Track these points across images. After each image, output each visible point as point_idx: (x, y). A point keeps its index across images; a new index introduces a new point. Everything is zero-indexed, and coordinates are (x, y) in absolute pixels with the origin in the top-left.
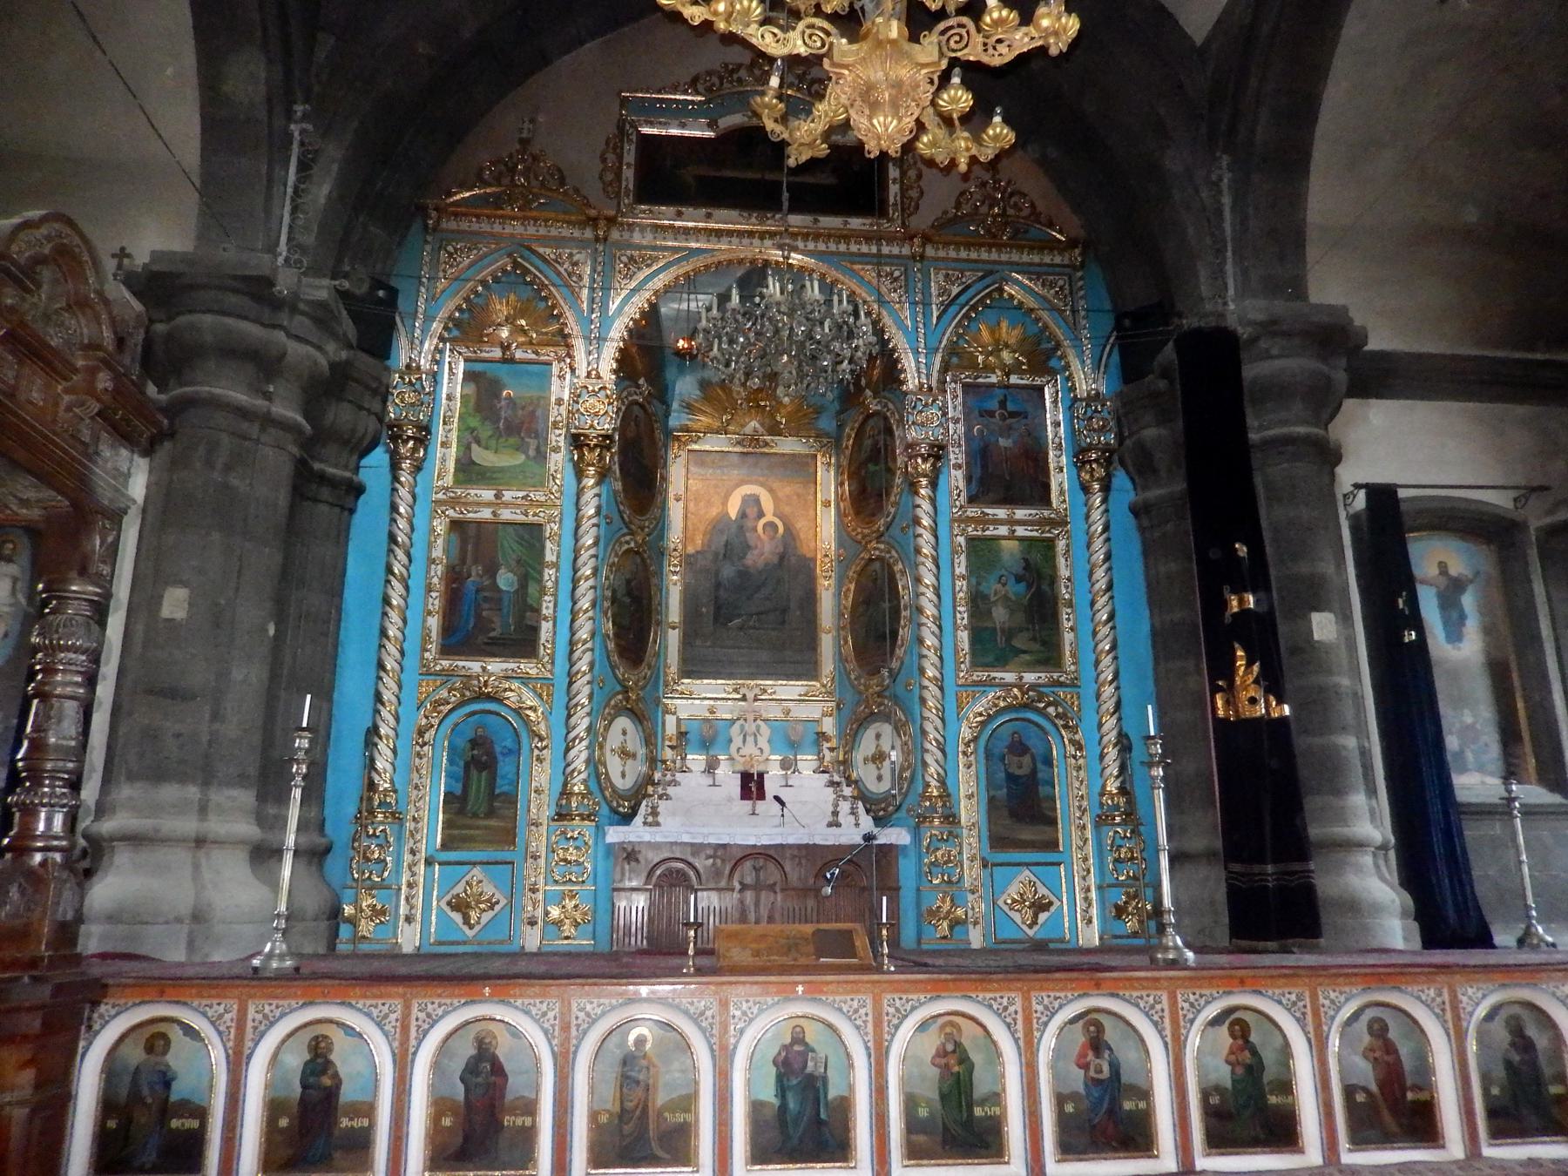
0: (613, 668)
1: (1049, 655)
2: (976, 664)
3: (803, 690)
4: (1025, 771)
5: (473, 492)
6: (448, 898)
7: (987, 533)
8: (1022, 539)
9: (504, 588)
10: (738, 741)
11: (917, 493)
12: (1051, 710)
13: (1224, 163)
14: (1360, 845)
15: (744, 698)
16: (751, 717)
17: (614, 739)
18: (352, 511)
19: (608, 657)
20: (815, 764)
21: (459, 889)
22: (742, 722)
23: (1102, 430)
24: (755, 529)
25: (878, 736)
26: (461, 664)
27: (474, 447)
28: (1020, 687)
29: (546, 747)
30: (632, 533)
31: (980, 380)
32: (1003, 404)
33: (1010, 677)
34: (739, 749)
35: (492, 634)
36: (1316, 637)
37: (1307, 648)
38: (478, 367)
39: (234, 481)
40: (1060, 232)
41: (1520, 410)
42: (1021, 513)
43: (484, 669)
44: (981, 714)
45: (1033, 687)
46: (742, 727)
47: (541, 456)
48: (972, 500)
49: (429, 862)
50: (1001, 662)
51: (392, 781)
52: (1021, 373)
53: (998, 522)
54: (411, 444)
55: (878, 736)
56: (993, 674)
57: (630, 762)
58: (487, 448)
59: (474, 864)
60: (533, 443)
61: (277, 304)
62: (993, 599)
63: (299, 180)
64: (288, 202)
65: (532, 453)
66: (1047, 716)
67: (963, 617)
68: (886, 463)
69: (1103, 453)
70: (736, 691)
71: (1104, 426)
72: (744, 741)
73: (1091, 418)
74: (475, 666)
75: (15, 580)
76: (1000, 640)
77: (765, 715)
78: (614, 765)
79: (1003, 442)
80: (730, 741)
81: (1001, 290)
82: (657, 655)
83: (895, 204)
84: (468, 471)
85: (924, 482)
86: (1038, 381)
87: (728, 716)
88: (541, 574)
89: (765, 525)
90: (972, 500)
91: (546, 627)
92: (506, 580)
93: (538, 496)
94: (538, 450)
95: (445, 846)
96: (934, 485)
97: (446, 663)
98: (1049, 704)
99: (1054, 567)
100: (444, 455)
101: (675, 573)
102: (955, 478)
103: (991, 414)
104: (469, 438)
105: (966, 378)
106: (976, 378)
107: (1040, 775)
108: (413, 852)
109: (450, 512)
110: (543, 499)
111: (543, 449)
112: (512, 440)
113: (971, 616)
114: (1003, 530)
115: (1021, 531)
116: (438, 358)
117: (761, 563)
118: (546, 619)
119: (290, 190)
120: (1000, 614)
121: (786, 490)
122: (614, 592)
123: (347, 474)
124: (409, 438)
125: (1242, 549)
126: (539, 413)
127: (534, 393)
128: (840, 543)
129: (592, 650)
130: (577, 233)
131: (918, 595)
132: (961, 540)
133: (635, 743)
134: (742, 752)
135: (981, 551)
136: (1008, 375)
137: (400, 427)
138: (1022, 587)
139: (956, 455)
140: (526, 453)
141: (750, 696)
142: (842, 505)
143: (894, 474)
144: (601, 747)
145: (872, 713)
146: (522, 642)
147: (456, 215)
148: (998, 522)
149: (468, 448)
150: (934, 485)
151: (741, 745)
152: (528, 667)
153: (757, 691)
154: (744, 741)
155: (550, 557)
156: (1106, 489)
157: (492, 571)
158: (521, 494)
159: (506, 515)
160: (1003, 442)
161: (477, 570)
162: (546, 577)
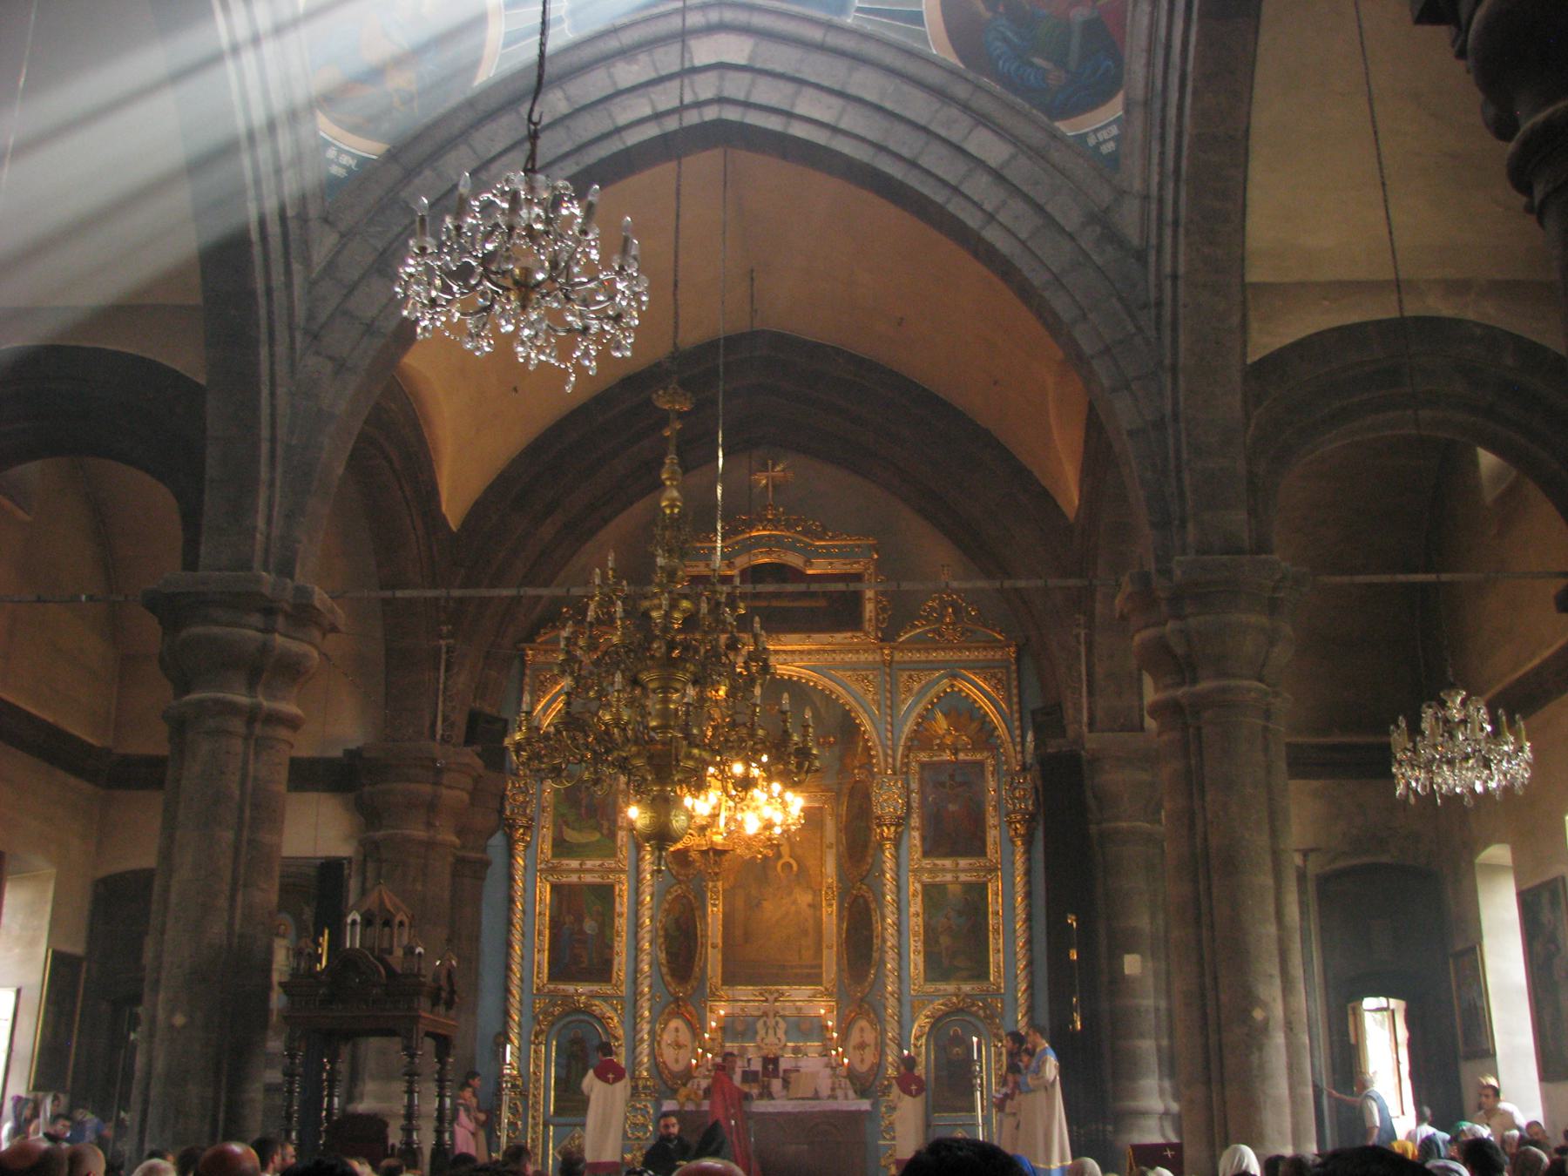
0: (666, 985)
1: (979, 971)
3: (809, 993)
5: (565, 862)
6: (559, 1148)
7: (937, 879)
8: (964, 884)
9: (589, 932)
10: (762, 1032)
11: (883, 852)
12: (981, 1013)
13: (1082, 621)
14: (1144, 1113)
15: (766, 1001)
16: (771, 1014)
17: (667, 1037)
18: (483, 879)
19: (663, 979)
20: (820, 1049)
21: (566, 1142)
22: (765, 1018)
23: (1023, 799)
24: (776, 868)
26: (562, 987)
27: (564, 827)
28: (957, 996)
29: (620, 1045)
30: (680, 882)
31: (935, 759)
32: (952, 776)
33: (950, 988)
34: (763, 1039)
35: (583, 965)
36: (1127, 971)
37: (1117, 979)
39: (419, 887)
40: (1000, 634)
41: (1315, 784)
42: (963, 863)
45: (967, 995)
46: (765, 1023)
48: (926, 854)
49: (546, 1125)
50: (945, 976)
51: (519, 1071)
52: (965, 750)
53: (944, 870)
54: (521, 831)
57: (682, 1051)
58: (573, 829)
59: (575, 1125)
60: (606, 824)
61: (439, 772)
62: (940, 930)
63: (447, 679)
64: (441, 693)
65: (605, 831)
69: (1024, 815)
70: (761, 994)
71: (1025, 794)
72: (767, 1033)
73: (1015, 789)
74: (570, 988)
75: (288, 949)
77: (782, 1013)
78: (668, 1055)
79: (952, 807)
80: (756, 1032)
81: (952, 686)
82: (704, 970)
83: (870, 620)
84: (562, 847)
85: (888, 845)
86: (979, 757)
87: (756, 1013)
88: (613, 921)
89: (784, 864)
90: (926, 854)
92: (589, 926)
93: (610, 863)
94: (609, 829)
95: (555, 1111)
96: (897, 844)
97: (551, 987)
100: (546, 834)
101: (715, 905)
103: (943, 785)
104: (560, 823)
105: (924, 757)
106: (931, 757)
108: (534, 1118)
109: (550, 878)
110: (613, 866)
113: (926, 942)
119: (441, 686)
120: (945, 940)
122: (666, 930)
123: (479, 855)
124: (521, 827)
125: (1071, 920)
128: (840, 880)
131: (884, 929)
132: (918, 886)
133: (685, 1036)
134: (767, 1041)
135: (933, 894)
136: (955, 754)
137: (514, 820)
139: (915, 821)
140: (600, 832)
141: (771, 998)
144: (659, 1043)
146: (602, 971)
147: (546, 651)
148: (944, 870)
149: (561, 832)
150: (897, 844)
151: (764, 1035)
152: (607, 989)
153: (776, 995)
154: (767, 1033)
155: (618, 908)
156: (1029, 842)
157: (579, 919)
158: (598, 863)
159: (588, 878)
160: (952, 807)
161: (569, 919)
162: (617, 923)
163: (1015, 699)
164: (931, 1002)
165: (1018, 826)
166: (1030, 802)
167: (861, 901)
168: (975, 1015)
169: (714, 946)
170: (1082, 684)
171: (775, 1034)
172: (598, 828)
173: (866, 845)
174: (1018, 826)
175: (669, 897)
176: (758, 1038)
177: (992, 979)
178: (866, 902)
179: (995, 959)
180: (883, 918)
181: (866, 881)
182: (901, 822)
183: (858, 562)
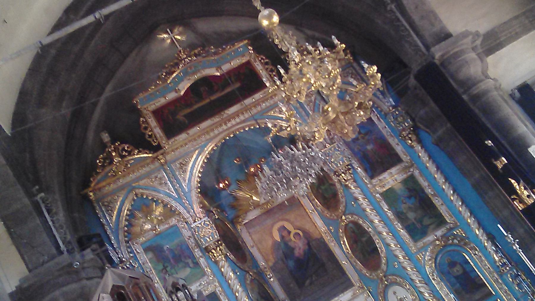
2: (415, 241)
4: (461, 272)
12: (456, 241)
25: (395, 293)
28: (438, 240)
33: (430, 238)
38: (148, 244)
44: (430, 260)
47: (197, 264)
50: (424, 233)
55: (395, 293)
56: (424, 241)
60: (190, 261)
65: (191, 265)
66: (456, 245)
67: (399, 226)
68: (328, 182)
76: (418, 225)
90: (372, 177)
94: (194, 263)
98: (453, 240)
99: (419, 185)
107: (468, 269)
111: (195, 261)
112: (181, 265)
116: (129, 250)
117: (302, 252)
120: (411, 215)
121: (292, 216)
126: (184, 247)
127: (176, 241)
130: (152, 166)
132: (378, 195)
138: (413, 200)
142: (319, 209)
143: (335, 185)
145: (386, 285)
158: (198, 284)
164: (426, 251)
166: (409, 120)
167: (351, 225)
168: (452, 244)
170: (409, 32)
172: (187, 265)
173: (335, 195)
174: (410, 136)
175: (248, 282)
177: (449, 221)
178: (356, 224)
179: (443, 210)
180: (372, 222)
181: (347, 212)
182: (349, 168)
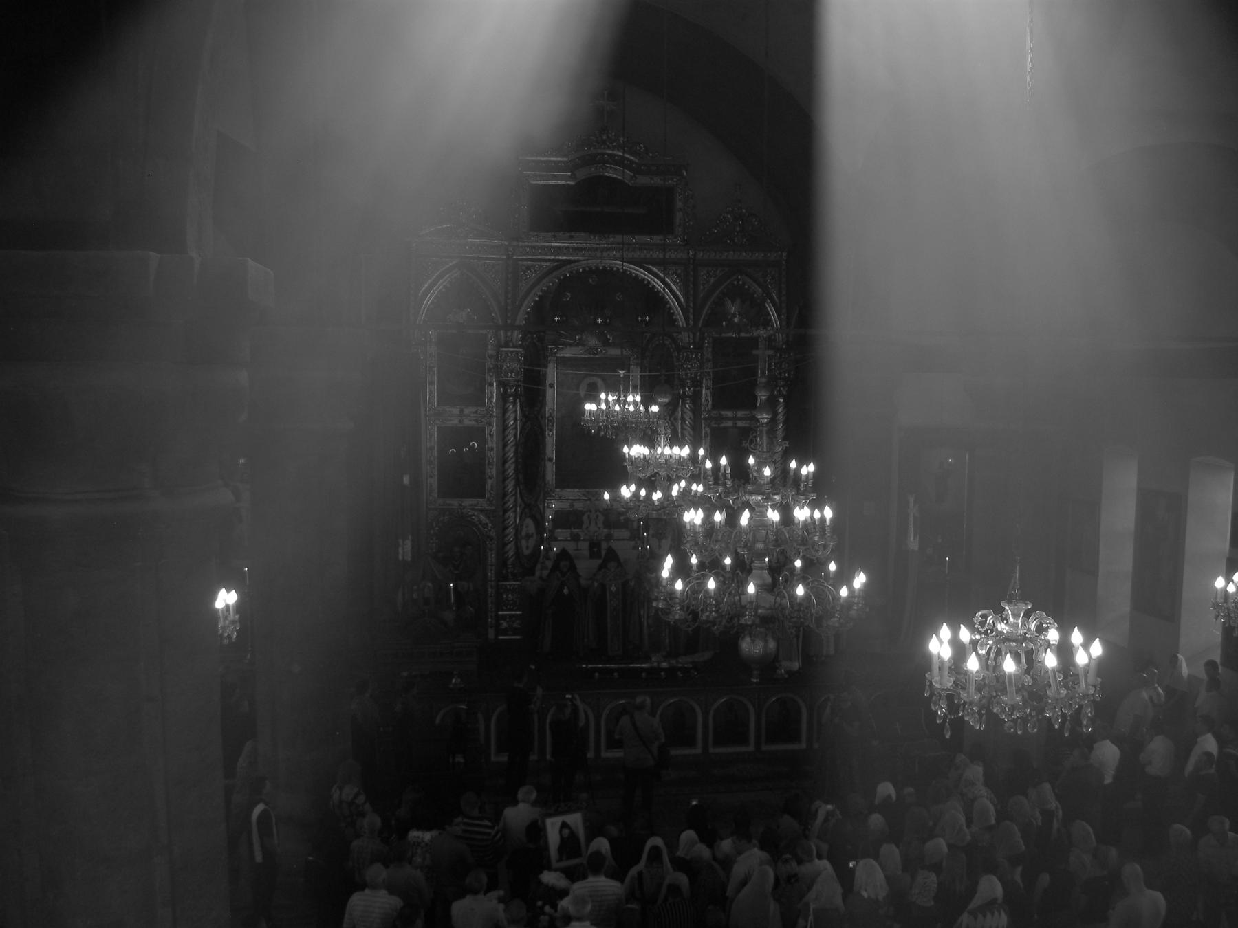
15: (590, 500)
22: (589, 513)
42: (740, 414)
43: (460, 505)
46: (589, 516)
48: (714, 407)
53: (728, 419)
70: (584, 495)
91: (489, 482)
102: (706, 394)
114: (730, 424)
115: (740, 424)
118: (490, 478)
129: (514, 495)
132: (708, 430)
148: (728, 419)
154: (590, 523)
163: (784, 292)
165: (782, 388)
169: (550, 460)
171: (596, 523)
176: (584, 527)
183: (672, 179)
